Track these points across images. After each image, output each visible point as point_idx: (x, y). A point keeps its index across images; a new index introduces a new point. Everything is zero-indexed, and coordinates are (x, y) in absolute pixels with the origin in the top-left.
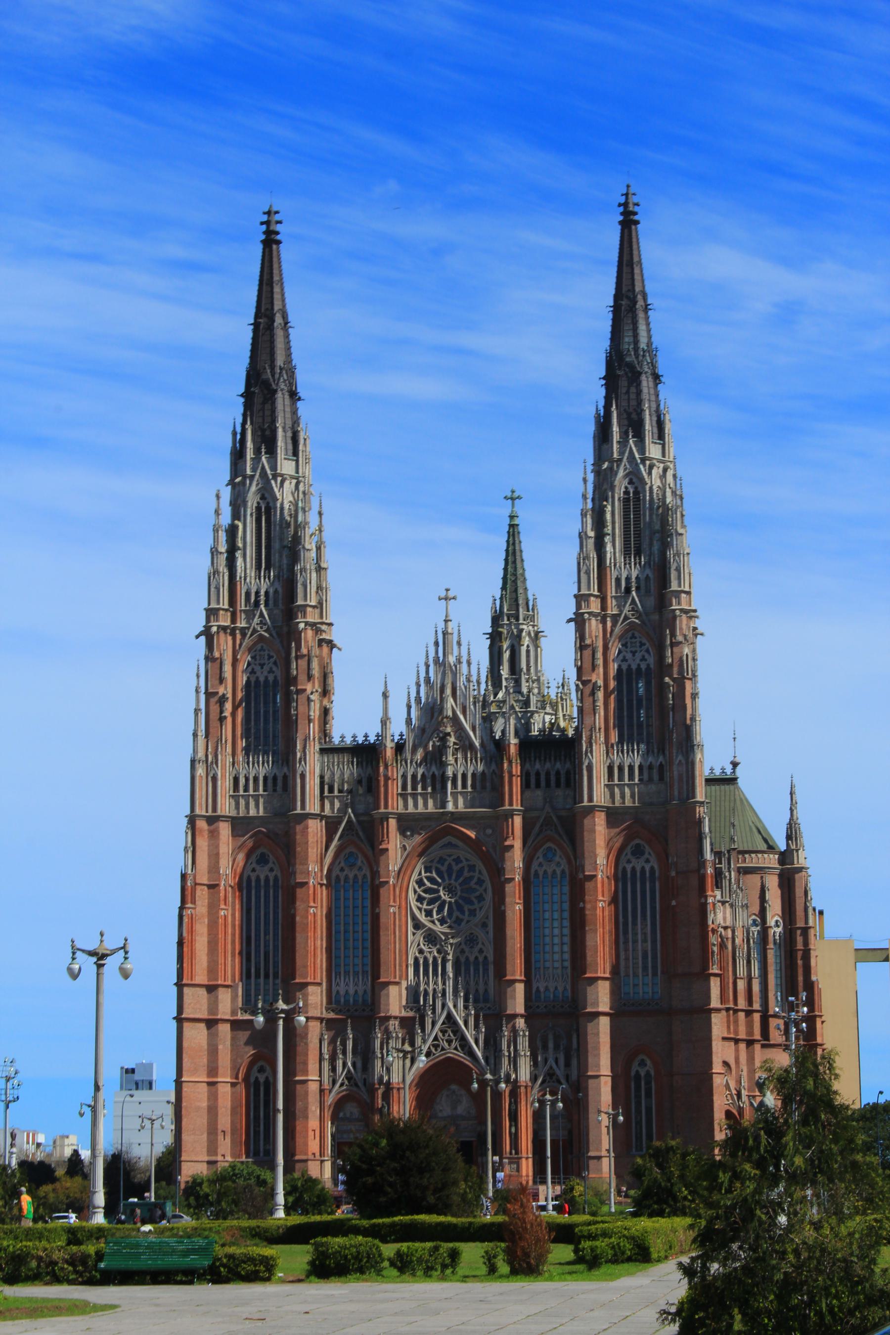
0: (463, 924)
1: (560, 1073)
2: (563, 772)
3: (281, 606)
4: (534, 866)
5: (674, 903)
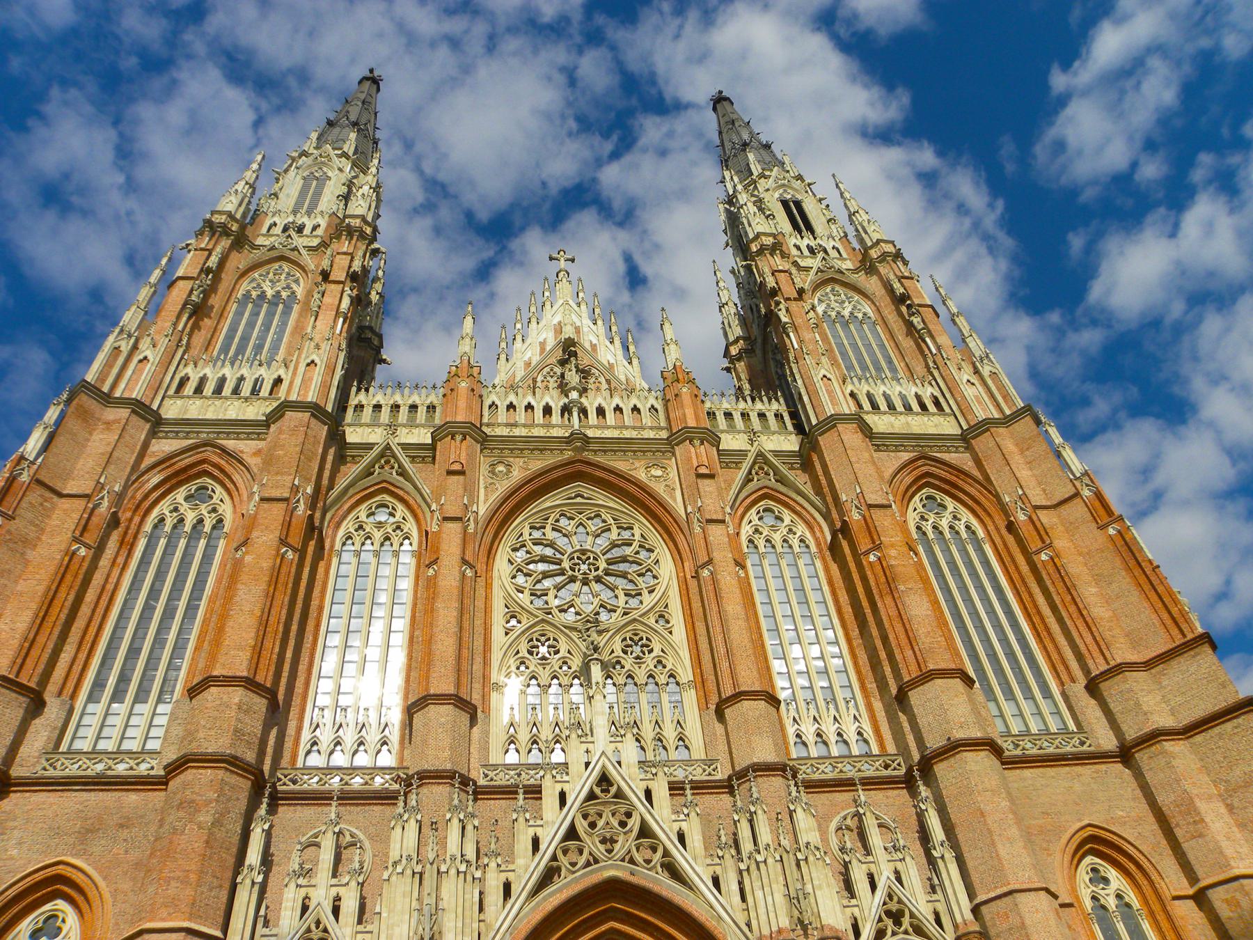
0: (614, 615)
1: (920, 903)
4: (746, 530)
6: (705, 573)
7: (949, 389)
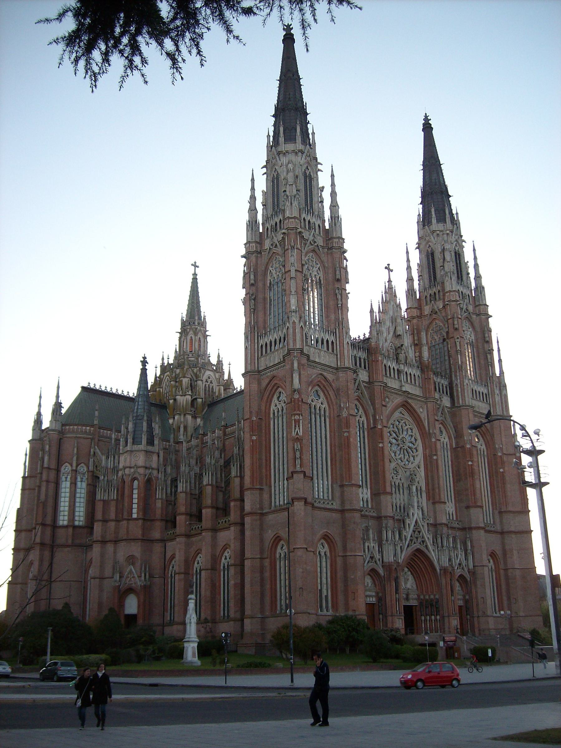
1: (464, 563)
2: (444, 386)
3: (322, 234)
5: (501, 470)
6: (435, 457)
7: (491, 392)
